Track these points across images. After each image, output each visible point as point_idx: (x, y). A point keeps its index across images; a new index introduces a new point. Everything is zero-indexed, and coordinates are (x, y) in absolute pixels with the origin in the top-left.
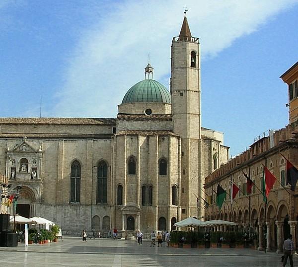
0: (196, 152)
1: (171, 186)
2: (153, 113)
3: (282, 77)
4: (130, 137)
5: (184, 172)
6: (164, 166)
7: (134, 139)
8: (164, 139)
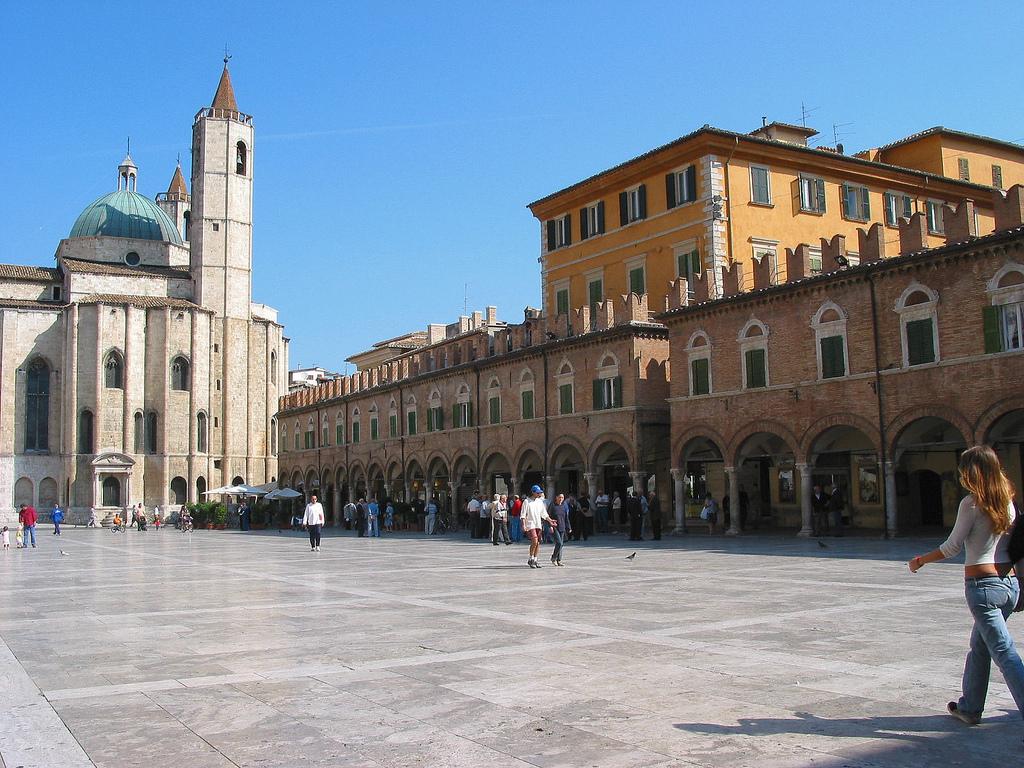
0: (242, 346)
1: (195, 414)
2: (141, 262)
3: (530, 206)
5: (222, 385)
6: (184, 368)
8: (181, 316)
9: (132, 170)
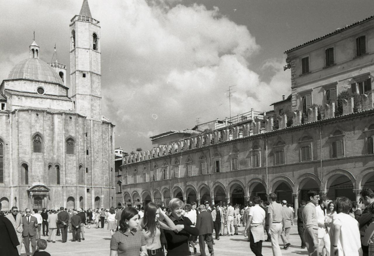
4: (35, 113)
7: (39, 116)
8: (71, 118)
9: (35, 48)
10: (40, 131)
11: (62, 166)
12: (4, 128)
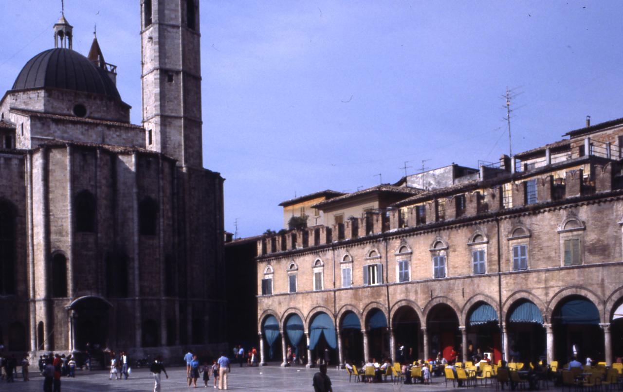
10: (90, 188)
11: (133, 259)
12: (15, 183)
